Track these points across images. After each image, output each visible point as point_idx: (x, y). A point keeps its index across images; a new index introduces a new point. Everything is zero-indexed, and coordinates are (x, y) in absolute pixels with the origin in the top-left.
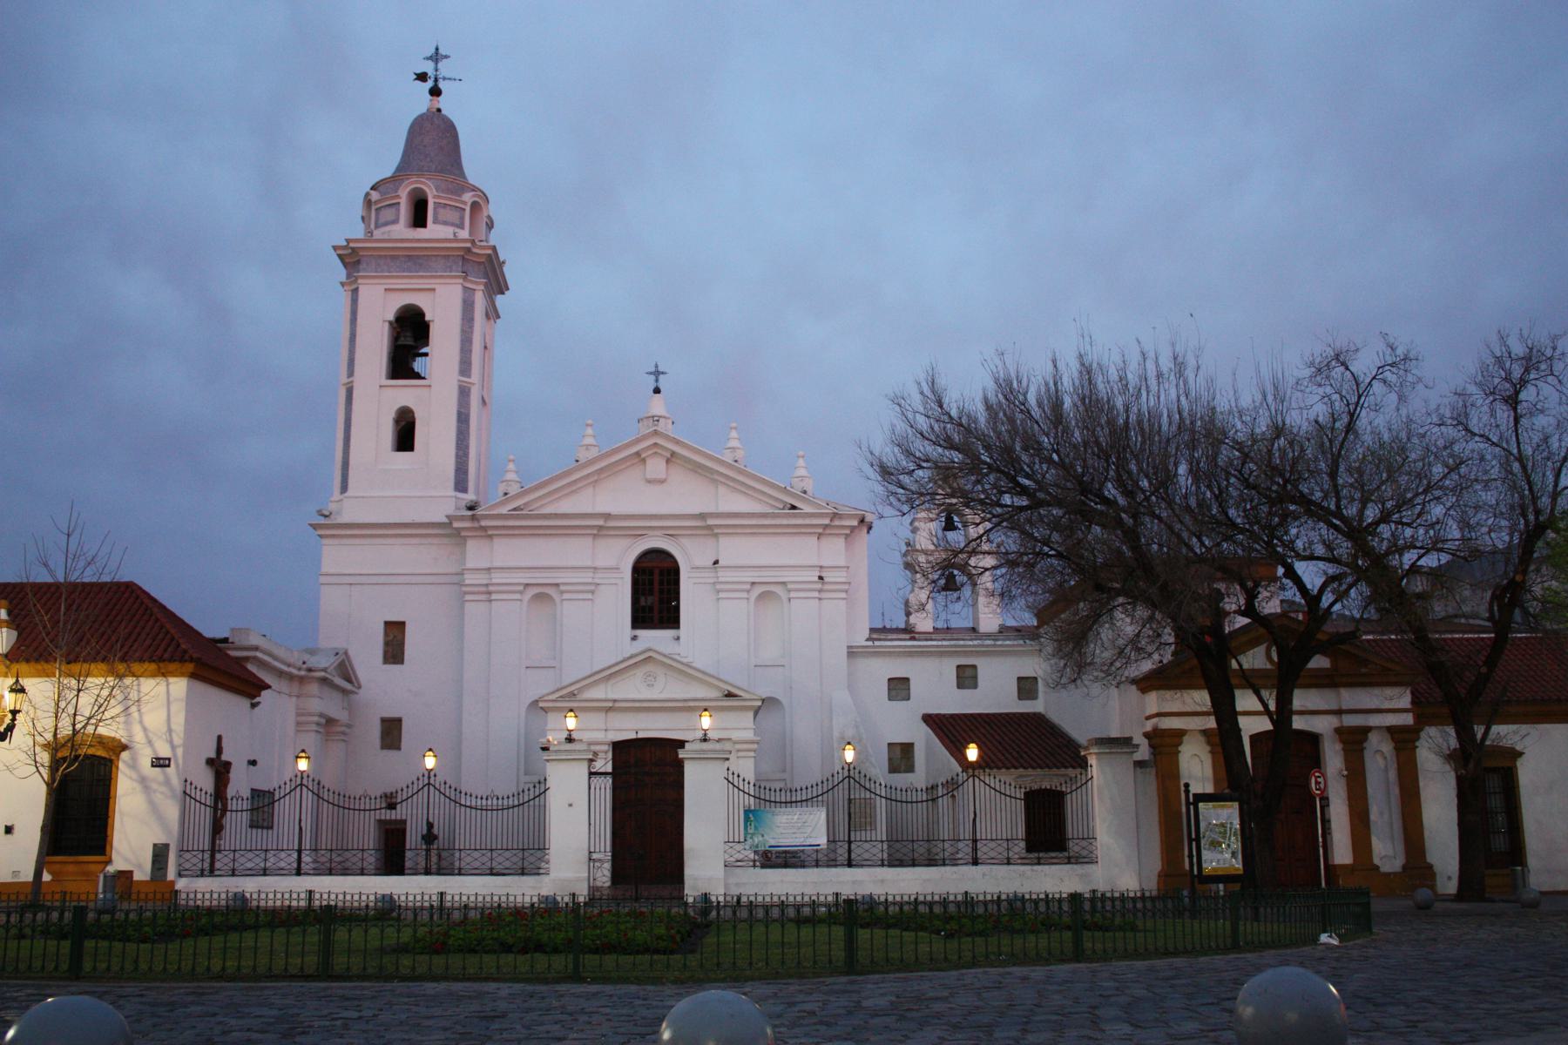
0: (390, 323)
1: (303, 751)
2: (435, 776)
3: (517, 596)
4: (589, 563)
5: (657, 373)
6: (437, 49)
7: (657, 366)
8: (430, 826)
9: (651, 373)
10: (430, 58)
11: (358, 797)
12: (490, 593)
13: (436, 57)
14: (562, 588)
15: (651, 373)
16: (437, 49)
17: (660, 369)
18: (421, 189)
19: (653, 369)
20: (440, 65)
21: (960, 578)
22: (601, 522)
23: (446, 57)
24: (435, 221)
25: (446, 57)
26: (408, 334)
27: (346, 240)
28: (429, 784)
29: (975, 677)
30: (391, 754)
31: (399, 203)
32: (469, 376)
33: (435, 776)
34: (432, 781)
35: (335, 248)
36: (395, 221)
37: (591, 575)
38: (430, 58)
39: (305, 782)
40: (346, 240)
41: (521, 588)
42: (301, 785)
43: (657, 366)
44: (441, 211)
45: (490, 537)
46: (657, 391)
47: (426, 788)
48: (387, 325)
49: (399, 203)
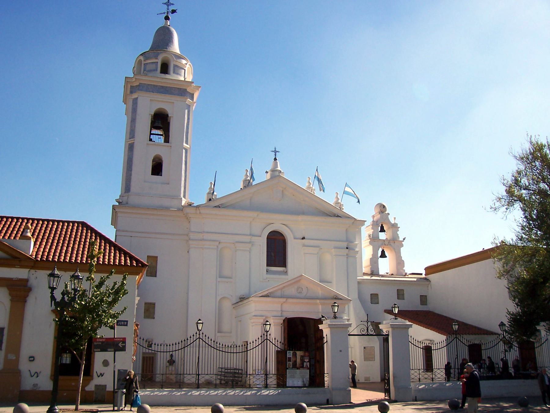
0: (151, 115)
1: (200, 320)
2: (270, 335)
5: (275, 152)
7: (275, 149)
8: (172, 356)
9: (273, 151)
10: (165, 4)
11: (230, 346)
13: (168, 4)
15: (273, 151)
17: (277, 150)
18: (168, 57)
19: (274, 150)
20: (169, 7)
21: (386, 254)
23: (173, 4)
24: (174, 72)
25: (173, 4)
26: (160, 122)
28: (267, 339)
29: (403, 295)
30: (149, 321)
31: (157, 62)
33: (270, 335)
34: (268, 338)
38: (165, 4)
39: (201, 337)
42: (199, 338)
43: (275, 149)
46: (275, 159)
47: (266, 340)
48: (151, 116)
49: (157, 62)
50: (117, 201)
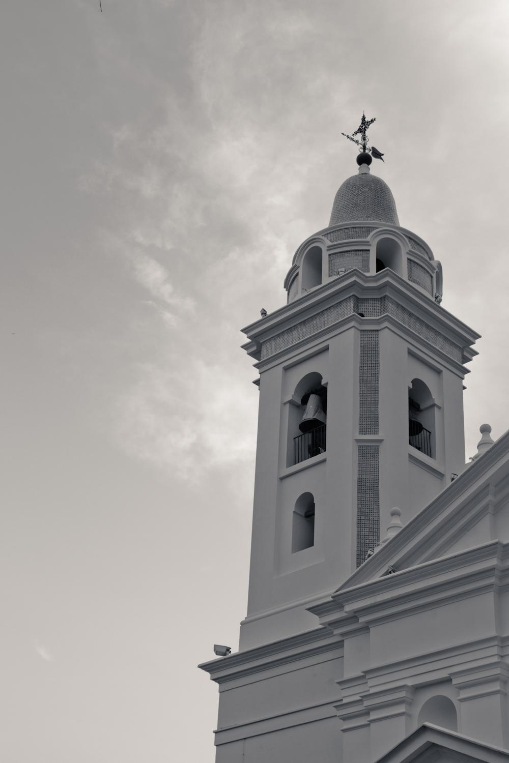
3: (401, 709)
4: (493, 633)
6: (364, 118)
12: (367, 713)
14: (454, 682)
16: (364, 118)
22: (493, 562)
25: (372, 121)
27: (245, 331)
32: (376, 433)
35: (245, 347)
36: (296, 293)
37: (495, 650)
40: (245, 331)
41: (402, 694)
44: (338, 261)
45: (366, 628)
48: (288, 405)
50: (218, 649)
